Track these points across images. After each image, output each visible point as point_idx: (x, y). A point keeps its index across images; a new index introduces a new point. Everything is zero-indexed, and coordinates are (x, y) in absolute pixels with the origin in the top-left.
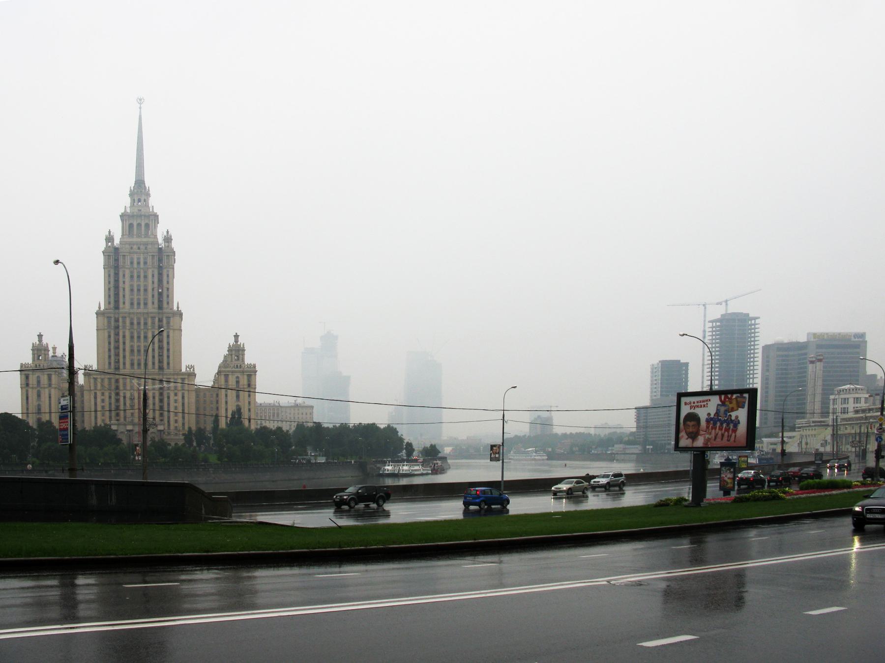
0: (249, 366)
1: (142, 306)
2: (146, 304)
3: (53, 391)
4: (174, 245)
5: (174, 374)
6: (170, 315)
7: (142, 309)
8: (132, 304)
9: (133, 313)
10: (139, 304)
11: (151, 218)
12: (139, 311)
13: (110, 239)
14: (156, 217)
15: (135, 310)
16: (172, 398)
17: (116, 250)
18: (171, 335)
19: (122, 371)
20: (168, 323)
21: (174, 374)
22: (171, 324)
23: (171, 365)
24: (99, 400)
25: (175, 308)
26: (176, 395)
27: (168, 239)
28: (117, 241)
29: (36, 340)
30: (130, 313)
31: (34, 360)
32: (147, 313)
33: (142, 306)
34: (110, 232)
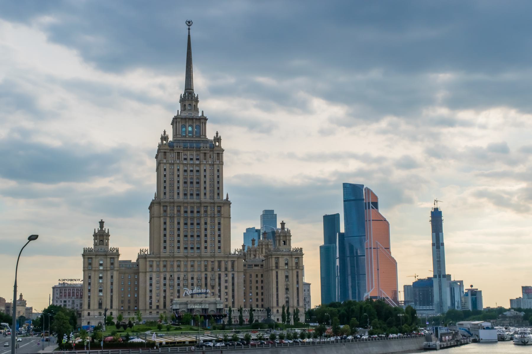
0: (296, 250)
1: (195, 196)
2: (198, 195)
3: (115, 274)
4: (223, 146)
5: (224, 257)
6: (221, 205)
7: (195, 199)
8: (185, 195)
9: (187, 203)
10: (192, 195)
11: (202, 121)
12: (192, 201)
13: (164, 138)
14: (203, 120)
15: (189, 199)
16: (223, 278)
17: (171, 145)
18: (222, 222)
19: (176, 254)
20: (219, 212)
21: (224, 257)
22: (222, 212)
23: (222, 248)
24: (154, 281)
25: (225, 198)
26: (226, 275)
27: (218, 139)
28: (171, 139)
29: (97, 227)
30: (184, 203)
31: (95, 245)
32: (200, 203)
33: (195, 196)
34: (165, 132)
